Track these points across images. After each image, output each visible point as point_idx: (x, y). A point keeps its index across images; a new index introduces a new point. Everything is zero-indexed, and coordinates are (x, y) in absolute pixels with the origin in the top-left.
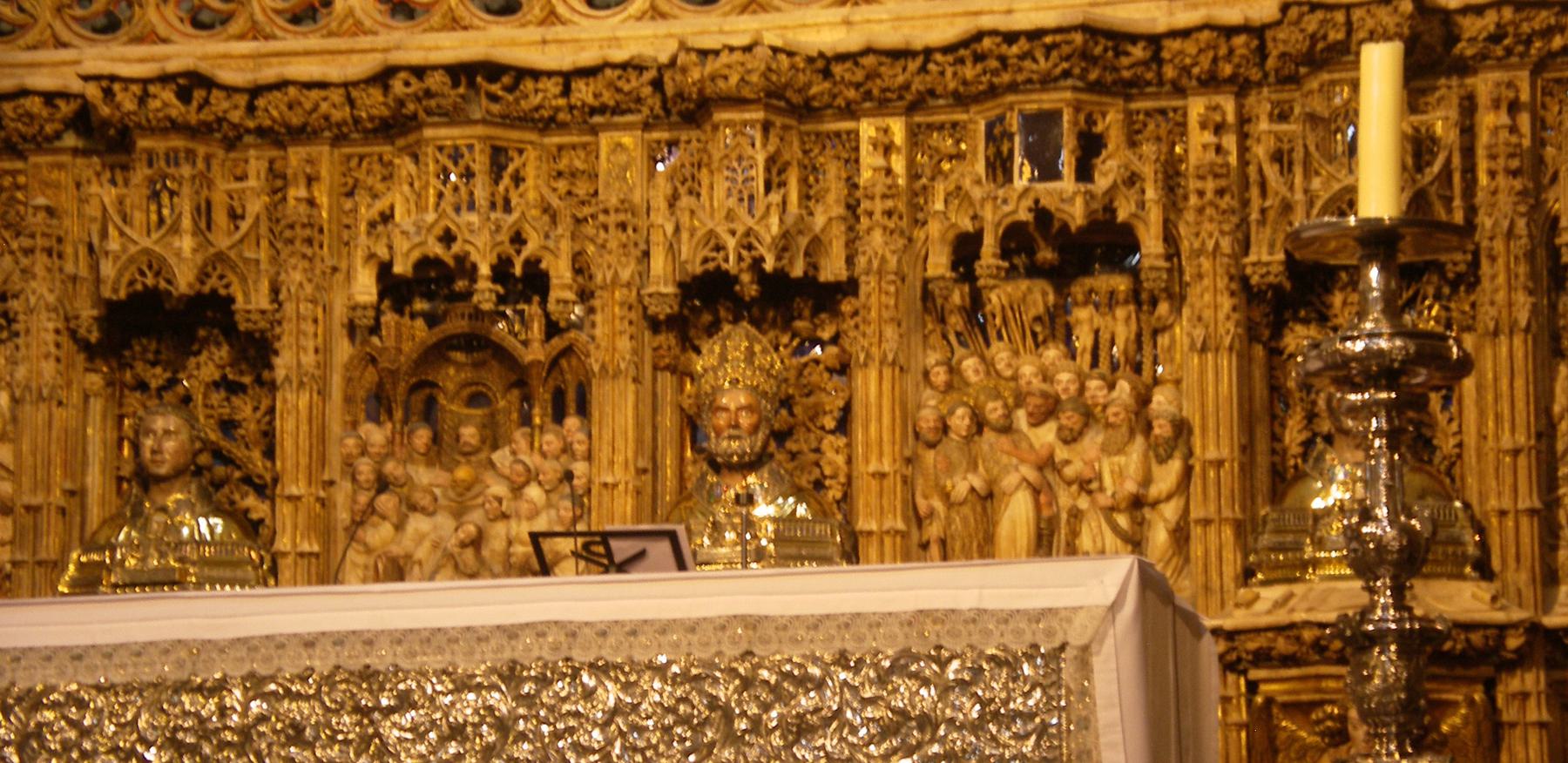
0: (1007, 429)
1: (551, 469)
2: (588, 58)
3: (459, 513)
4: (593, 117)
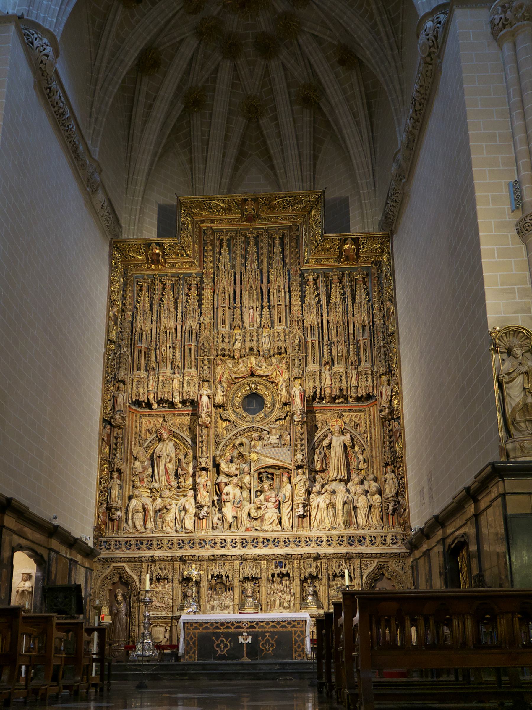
0: (276, 593)
1: (229, 596)
2: (234, 554)
3: (219, 600)
4: (234, 560)
